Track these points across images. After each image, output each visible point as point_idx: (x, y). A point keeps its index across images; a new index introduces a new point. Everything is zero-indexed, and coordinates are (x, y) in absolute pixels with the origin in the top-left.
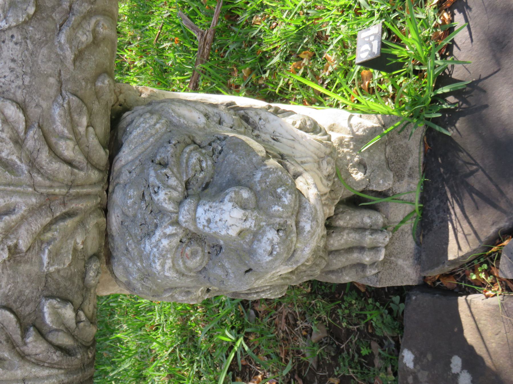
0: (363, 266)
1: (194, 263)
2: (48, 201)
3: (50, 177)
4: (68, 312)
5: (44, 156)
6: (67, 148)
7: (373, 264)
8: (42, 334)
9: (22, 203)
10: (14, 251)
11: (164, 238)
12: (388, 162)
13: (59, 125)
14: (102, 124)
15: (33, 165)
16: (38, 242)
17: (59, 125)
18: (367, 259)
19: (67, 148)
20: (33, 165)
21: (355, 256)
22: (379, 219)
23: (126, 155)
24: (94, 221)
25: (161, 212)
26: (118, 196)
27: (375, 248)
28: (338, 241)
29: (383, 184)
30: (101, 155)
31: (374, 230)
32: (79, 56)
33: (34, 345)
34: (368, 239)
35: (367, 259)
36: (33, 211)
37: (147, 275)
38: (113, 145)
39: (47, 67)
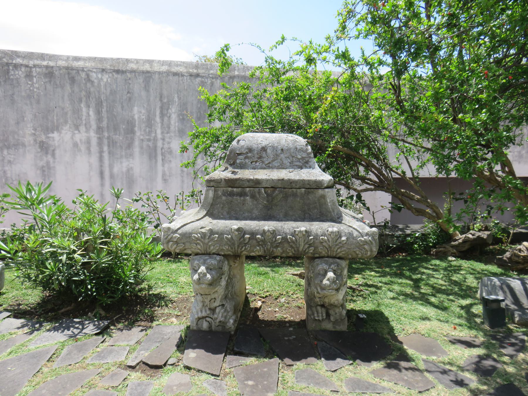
0: (313, 314)
1: (321, 272)
2: (330, 247)
3: (334, 248)
4: (311, 251)
5: (338, 247)
6: (339, 250)
7: (314, 317)
8: (309, 247)
9: (330, 244)
10: (322, 243)
11: (325, 267)
12: (337, 320)
13: (343, 249)
14: (343, 256)
15: (337, 245)
16: (324, 246)
17: (343, 249)
18: (316, 315)
19: (339, 250)
20: (337, 245)
21: (316, 313)
22: (325, 317)
23: (338, 260)
24: (326, 255)
25: (330, 266)
26: (331, 259)
27: (318, 316)
28: (319, 308)
29: (332, 319)
30: (338, 256)
31: (322, 316)
32: (354, 252)
33: (307, 246)
34: (320, 315)
35: (316, 315)
36: (329, 245)
37: (318, 265)
38: (339, 258)
39: (352, 247)
